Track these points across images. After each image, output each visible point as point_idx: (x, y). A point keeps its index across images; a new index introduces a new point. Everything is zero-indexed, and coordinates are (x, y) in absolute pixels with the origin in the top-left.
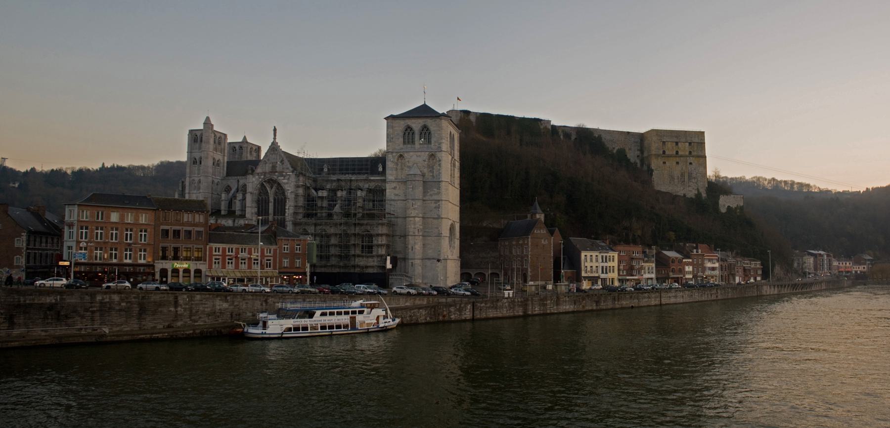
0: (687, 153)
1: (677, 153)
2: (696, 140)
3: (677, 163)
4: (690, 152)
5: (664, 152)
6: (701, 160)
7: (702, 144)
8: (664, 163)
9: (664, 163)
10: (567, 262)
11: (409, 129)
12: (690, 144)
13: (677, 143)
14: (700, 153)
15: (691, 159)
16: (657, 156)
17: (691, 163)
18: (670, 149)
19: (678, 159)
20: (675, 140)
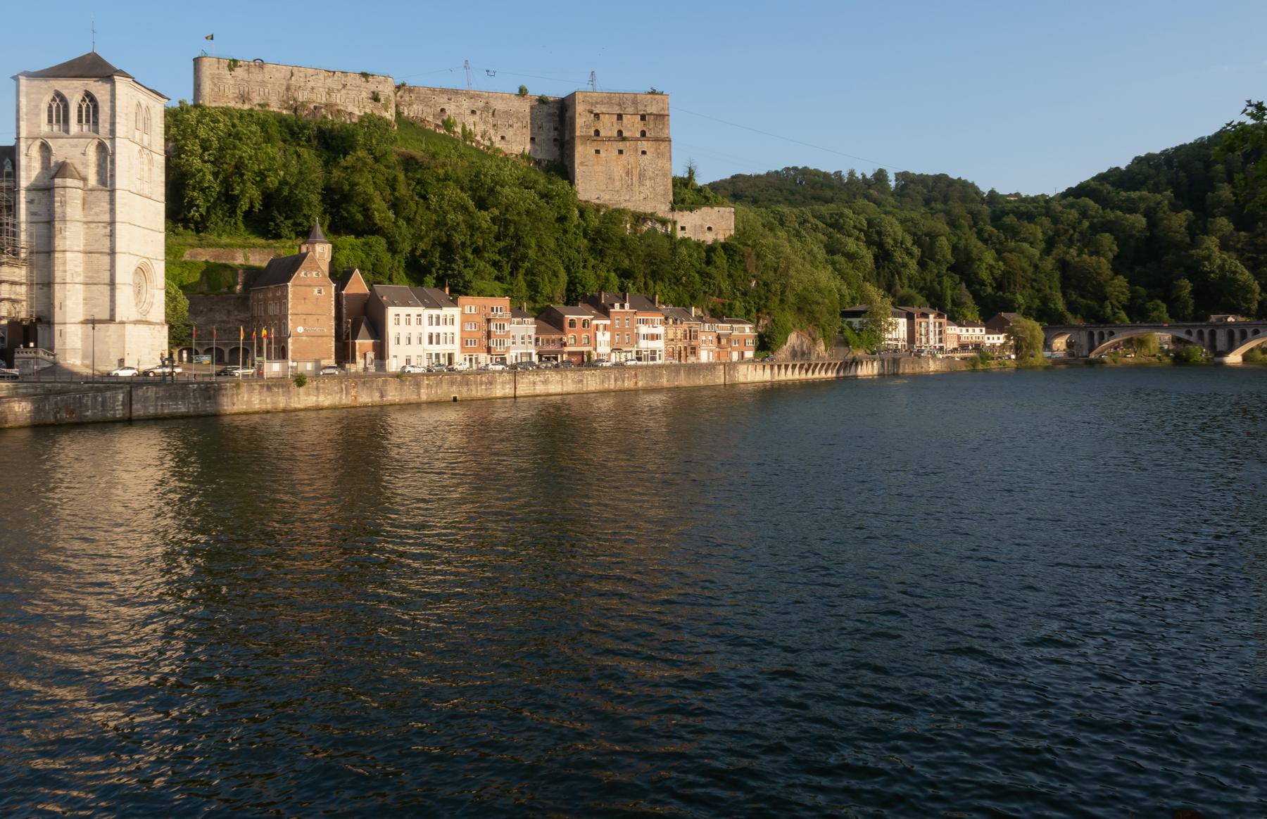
0: (638, 135)
1: (620, 132)
2: (653, 109)
3: (621, 152)
4: (643, 133)
5: (597, 133)
6: (664, 145)
7: (661, 117)
8: (598, 152)
9: (598, 152)
10: (360, 321)
11: (59, 96)
12: (643, 118)
13: (620, 117)
14: (663, 136)
15: (644, 145)
16: (586, 139)
17: (644, 153)
18: (608, 127)
19: (621, 145)
20: (617, 110)
